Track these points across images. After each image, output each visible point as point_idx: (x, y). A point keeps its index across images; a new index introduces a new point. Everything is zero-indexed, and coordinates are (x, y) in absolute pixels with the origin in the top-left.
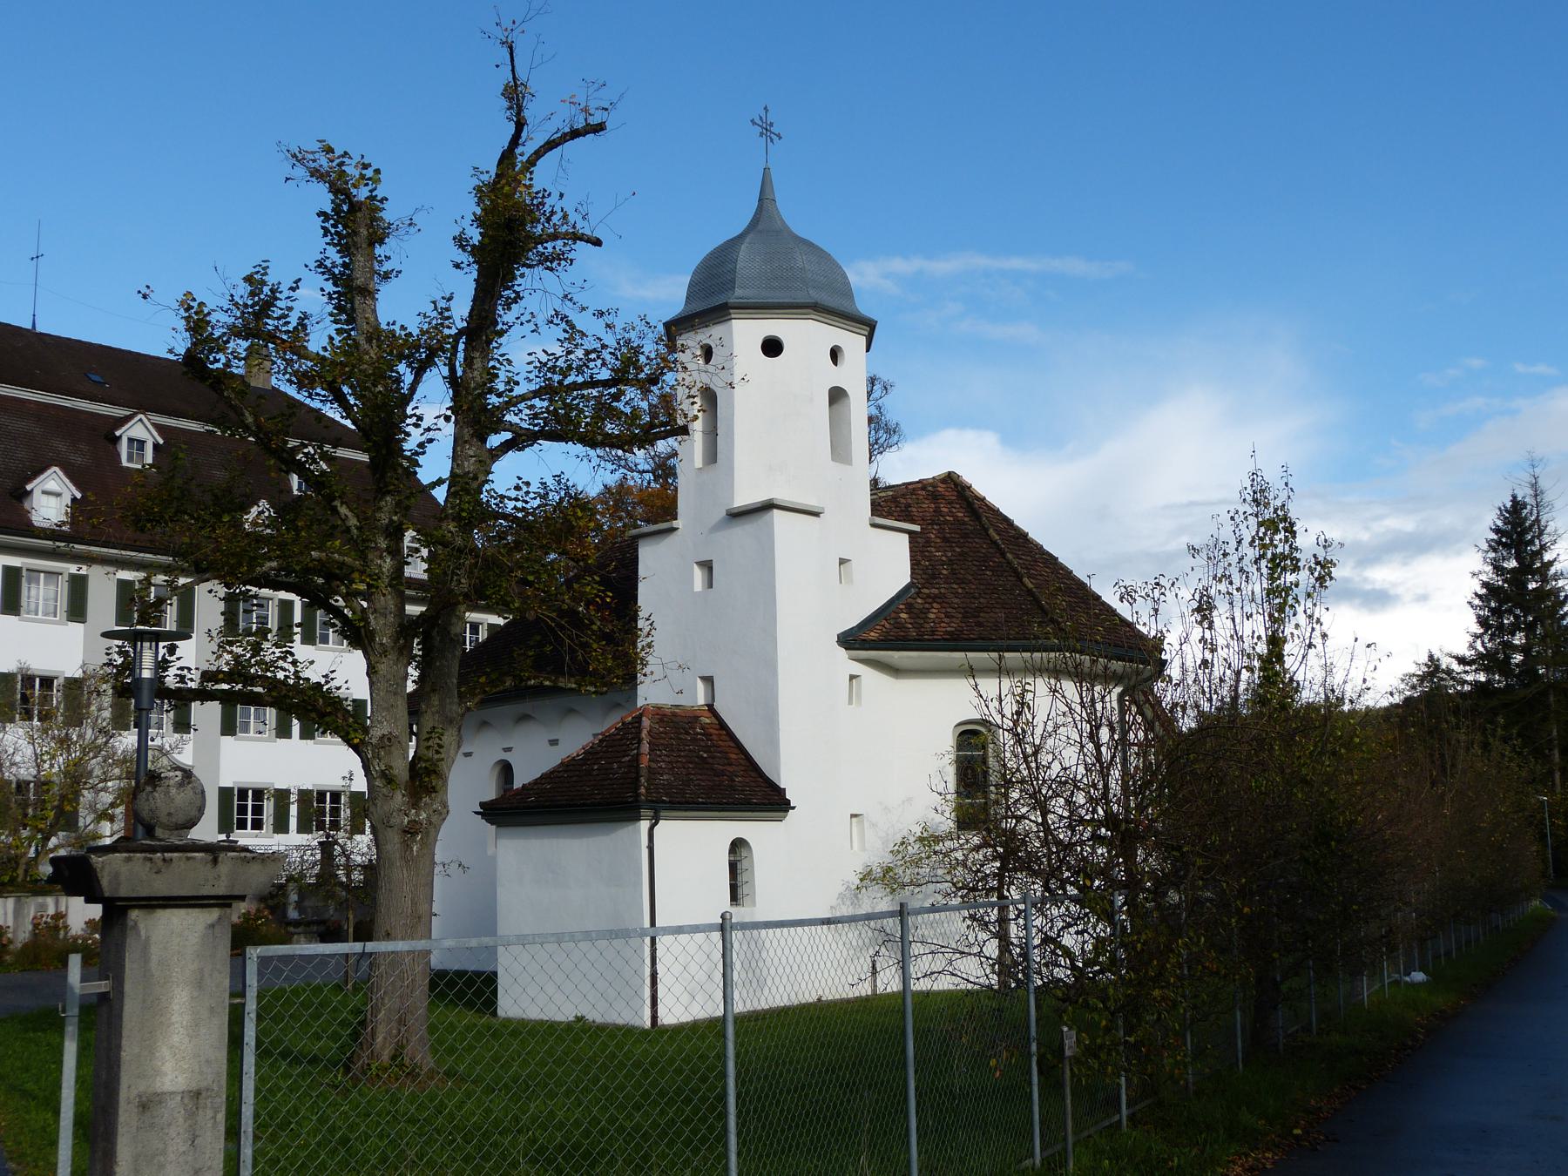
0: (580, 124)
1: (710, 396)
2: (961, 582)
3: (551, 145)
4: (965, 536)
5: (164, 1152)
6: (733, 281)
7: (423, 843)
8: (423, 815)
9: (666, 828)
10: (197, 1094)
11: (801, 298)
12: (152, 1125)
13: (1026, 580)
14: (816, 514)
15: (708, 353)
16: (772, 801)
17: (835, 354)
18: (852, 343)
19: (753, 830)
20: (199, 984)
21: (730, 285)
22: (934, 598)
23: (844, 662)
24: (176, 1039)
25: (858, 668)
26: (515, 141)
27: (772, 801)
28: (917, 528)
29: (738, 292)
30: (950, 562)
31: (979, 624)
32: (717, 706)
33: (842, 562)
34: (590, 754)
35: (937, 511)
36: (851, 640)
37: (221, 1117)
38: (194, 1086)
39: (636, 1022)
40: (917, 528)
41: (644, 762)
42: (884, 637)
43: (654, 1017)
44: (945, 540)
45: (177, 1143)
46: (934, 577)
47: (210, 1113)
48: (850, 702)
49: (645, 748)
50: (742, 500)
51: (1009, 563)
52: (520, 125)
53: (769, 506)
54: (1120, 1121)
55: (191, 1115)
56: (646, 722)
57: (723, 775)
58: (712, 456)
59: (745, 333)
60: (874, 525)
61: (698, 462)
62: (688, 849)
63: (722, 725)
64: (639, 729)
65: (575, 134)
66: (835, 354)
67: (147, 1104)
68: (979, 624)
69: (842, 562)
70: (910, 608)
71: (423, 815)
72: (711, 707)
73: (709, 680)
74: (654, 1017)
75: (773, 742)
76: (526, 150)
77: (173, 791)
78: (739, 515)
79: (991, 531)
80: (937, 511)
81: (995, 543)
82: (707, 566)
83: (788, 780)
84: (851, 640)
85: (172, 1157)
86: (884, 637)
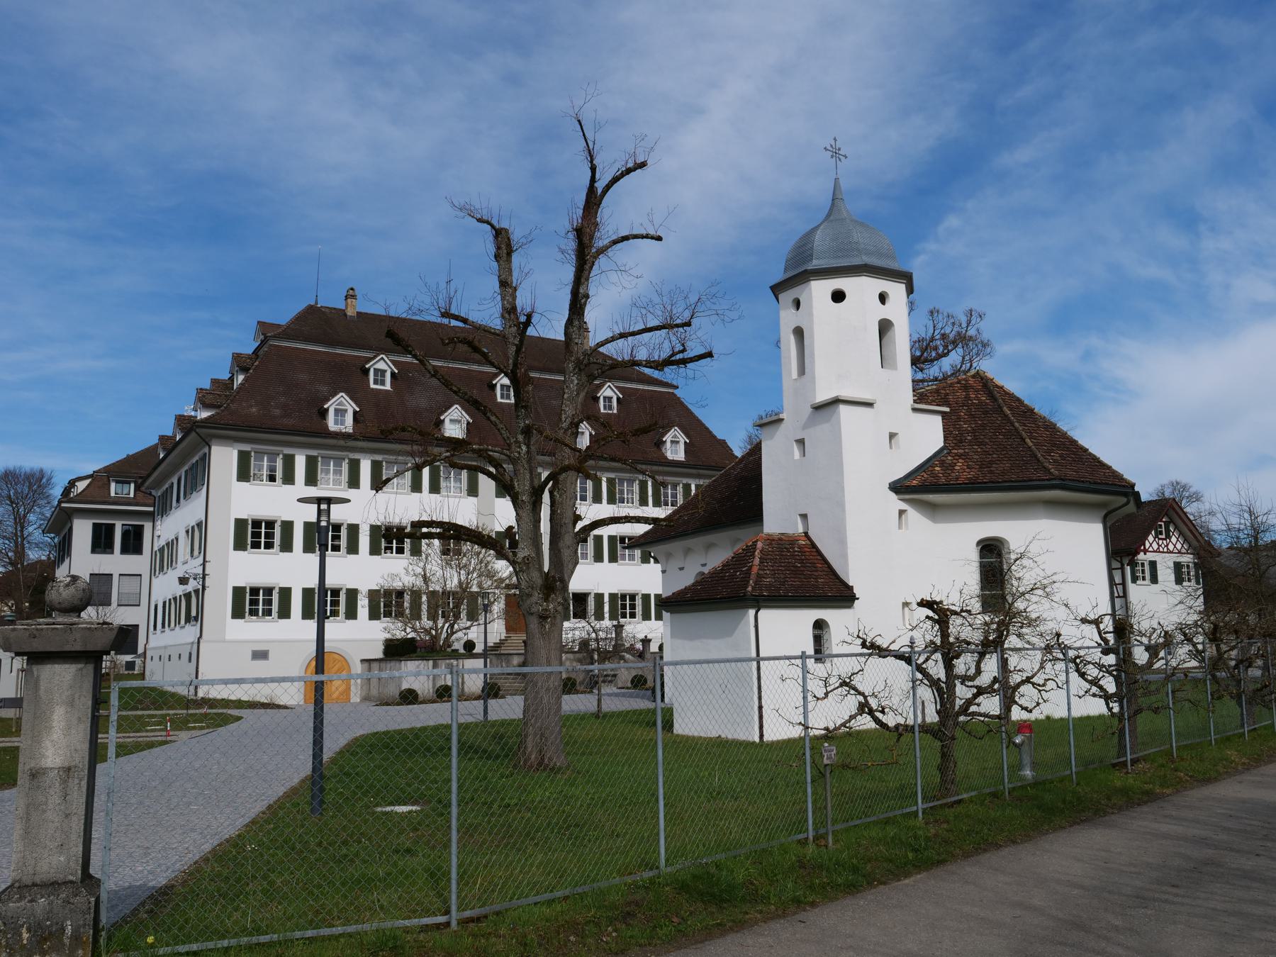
0: (630, 165)
1: (799, 332)
2: (981, 444)
3: (615, 180)
4: (986, 413)
5: (46, 804)
6: (811, 255)
7: (553, 624)
8: (551, 606)
9: (763, 613)
10: (69, 769)
11: (856, 261)
12: (38, 787)
13: (1028, 440)
14: (869, 405)
15: (797, 304)
16: (843, 596)
17: (883, 298)
18: (897, 290)
19: (831, 616)
20: (71, 703)
21: (810, 258)
22: (960, 456)
23: (895, 503)
24: (55, 736)
25: (904, 506)
26: (593, 180)
27: (843, 596)
28: (947, 409)
29: (815, 262)
30: (974, 431)
31: (991, 472)
32: (810, 533)
33: (892, 436)
34: (726, 566)
35: (967, 398)
36: (899, 488)
37: (84, 783)
38: (66, 764)
39: (750, 739)
40: (947, 409)
41: (755, 570)
42: (922, 487)
43: (761, 736)
44: (972, 416)
45: (54, 798)
46: (961, 441)
47: (76, 781)
48: (900, 527)
49: (757, 561)
50: (822, 396)
51: (1016, 429)
52: (593, 169)
53: (836, 401)
54: (917, 811)
55: (64, 782)
56: (760, 545)
57: (811, 579)
58: (802, 371)
59: (820, 290)
60: (914, 410)
61: (795, 374)
62: (785, 629)
63: (813, 545)
64: (755, 549)
65: (629, 171)
66: (883, 298)
67: (35, 775)
68: (991, 472)
69: (892, 436)
70: (942, 463)
71: (551, 606)
72: (806, 534)
73: (804, 517)
74: (761, 736)
75: (844, 556)
76: (600, 186)
77: (62, 589)
78: (819, 408)
79: (1005, 409)
80: (967, 398)
81: (1006, 416)
82: (801, 442)
83: (854, 579)
84: (899, 488)
85: (51, 806)
86: (922, 487)
